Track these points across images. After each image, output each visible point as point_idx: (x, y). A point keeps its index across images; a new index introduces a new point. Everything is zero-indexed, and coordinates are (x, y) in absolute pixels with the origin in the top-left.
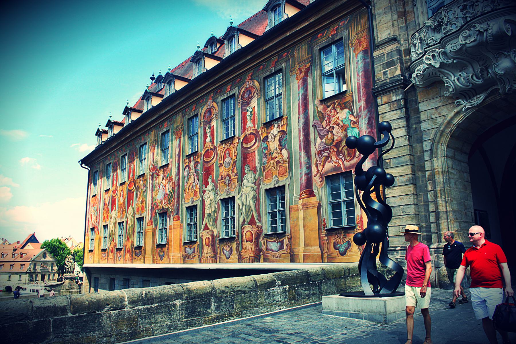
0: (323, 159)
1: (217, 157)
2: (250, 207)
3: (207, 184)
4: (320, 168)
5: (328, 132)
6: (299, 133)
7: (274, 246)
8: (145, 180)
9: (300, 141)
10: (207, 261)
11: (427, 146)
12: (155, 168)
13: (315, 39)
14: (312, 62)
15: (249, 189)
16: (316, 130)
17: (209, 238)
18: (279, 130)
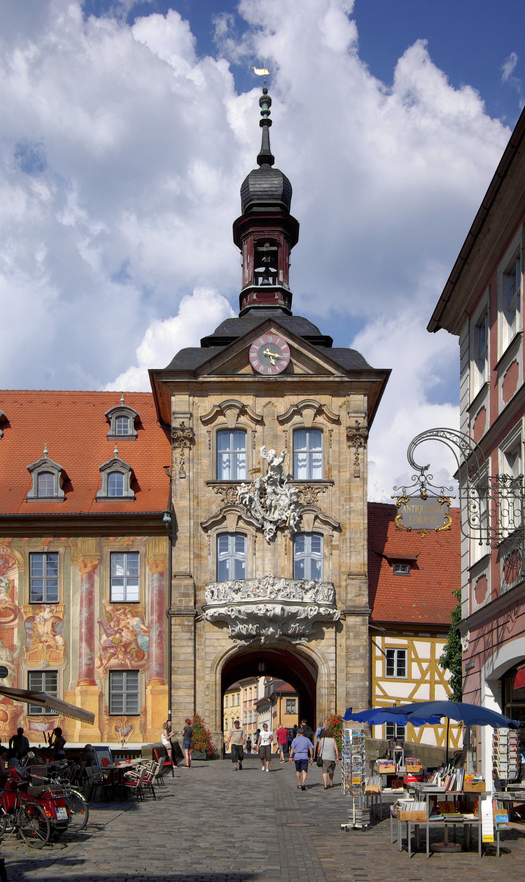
0: (108, 655)
4: (104, 662)
5: (116, 632)
6: (81, 624)
9: (81, 632)
11: (208, 664)
13: (106, 539)
14: (101, 561)
16: (102, 627)
18: (51, 615)
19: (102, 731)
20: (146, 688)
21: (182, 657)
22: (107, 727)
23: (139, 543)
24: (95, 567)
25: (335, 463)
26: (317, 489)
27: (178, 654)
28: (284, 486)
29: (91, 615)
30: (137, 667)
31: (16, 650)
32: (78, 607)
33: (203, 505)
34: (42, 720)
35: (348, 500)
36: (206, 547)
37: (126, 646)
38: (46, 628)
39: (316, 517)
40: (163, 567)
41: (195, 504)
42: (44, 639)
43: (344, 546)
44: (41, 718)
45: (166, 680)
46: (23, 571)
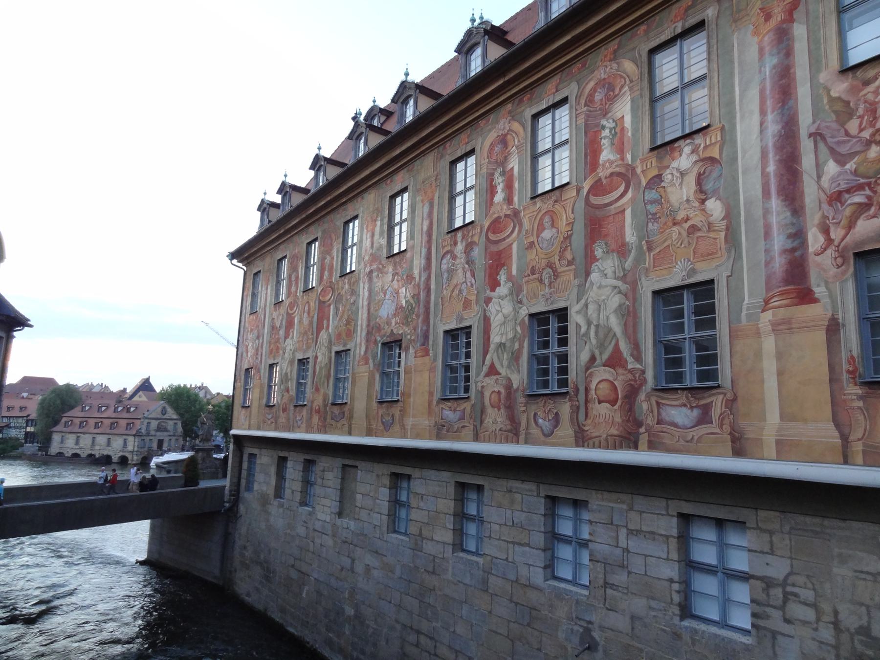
0: (848, 212)
1: (520, 231)
2: (610, 330)
3: (494, 284)
4: (836, 234)
7: (680, 414)
8: (354, 283)
9: (765, 175)
10: (493, 438)
12: (374, 258)
15: (607, 291)
16: (821, 145)
17: (499, 392)
18: (694, 158)
19: (846, 431)
22: (861, 418)
31: (630, 252)
32: (756, 118)
42: (680, 216)
44: (682, 397)
46: (639, 92)
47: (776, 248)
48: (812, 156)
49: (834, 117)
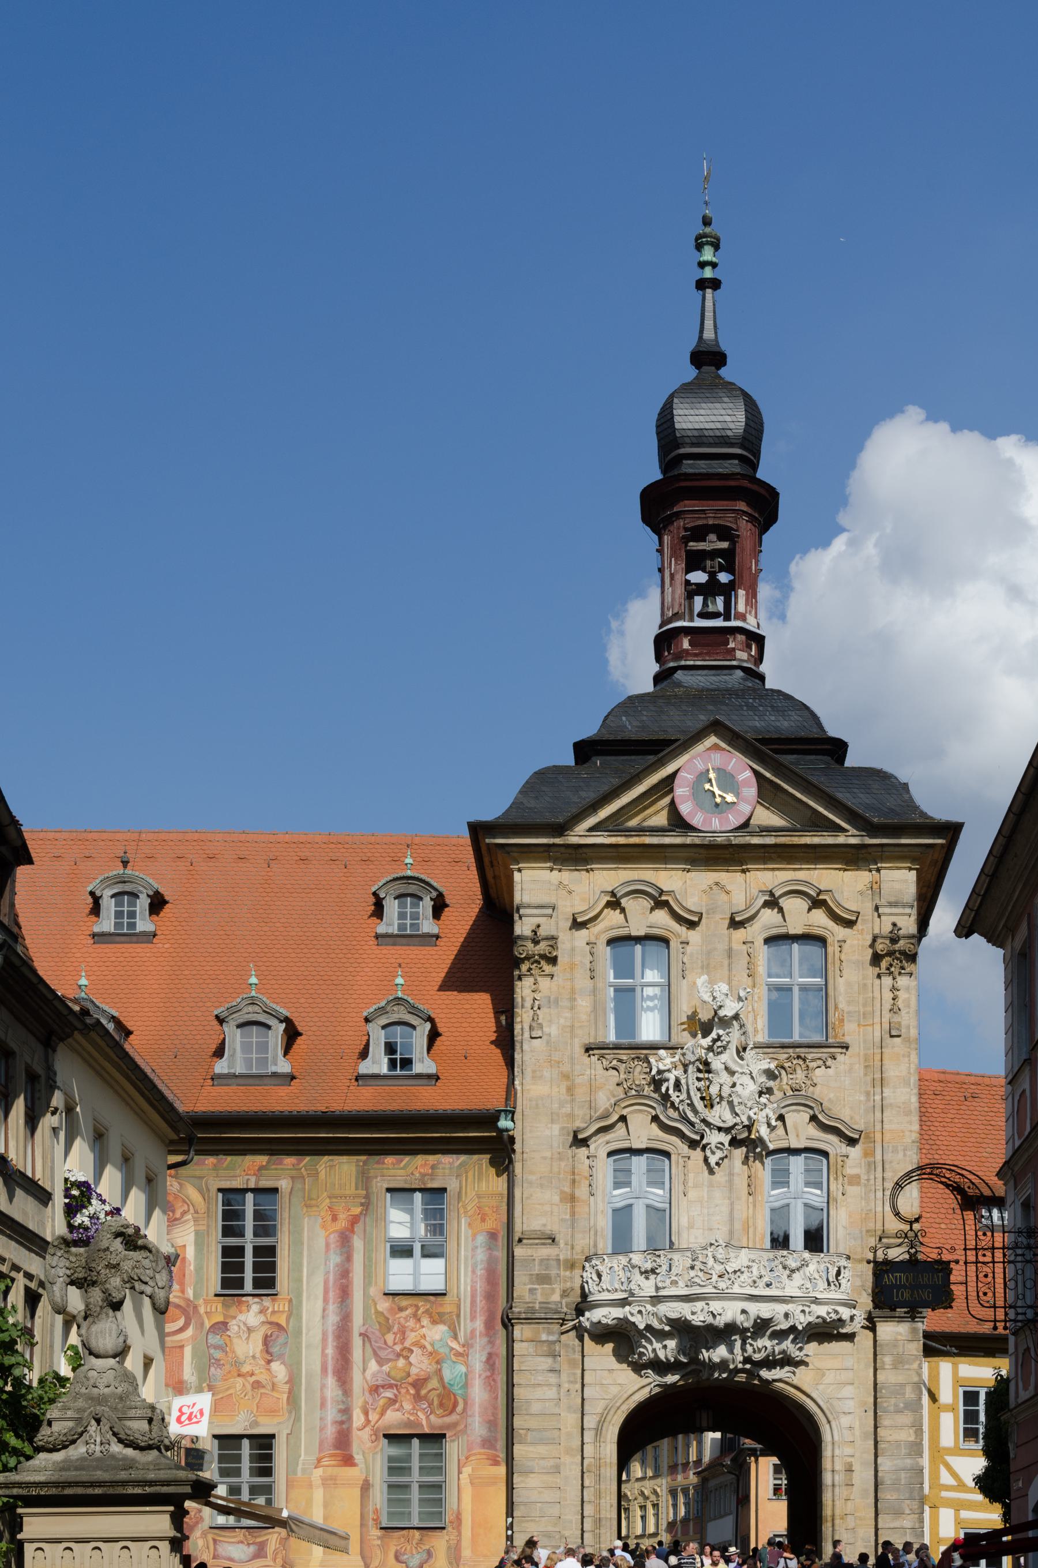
0: (382, 1402)
4: (373, 1417)
5: (399, 1355)
6: (324, 1340)
9: (324, 1354)
13: (378, 1163)
14: (367, 1205)
16: (367, 1345)
18: (262, 1318)
19: (368, 1561)
20: (460, 1472)
21: (535, 1408)
22: (379, 1552)
23: (447, 1171)
24: (354, 1220)
25: (851, 1008)
26: (813, 1060)
27: (528, 1402)
28: (749, 1054)
29: (346, 1319)
30: (441, 1428)
32: (320, 1304)
33: (581, 1094)
34: (241, 1538)
35: (878, 1083)
36: (586, 1178)
37: (418, 1384)
38: (251, 1345)
39: (814, 1118)
40: (496, 1221)
41: (564, 1090)
42: (246, 1368)
43: (872, 1177)
44: (240, 1534)
45: (502, 1455)
46: (205, 1228)
47: (329, 1418)
48: (361, 1351)
49: (378, 1327)
